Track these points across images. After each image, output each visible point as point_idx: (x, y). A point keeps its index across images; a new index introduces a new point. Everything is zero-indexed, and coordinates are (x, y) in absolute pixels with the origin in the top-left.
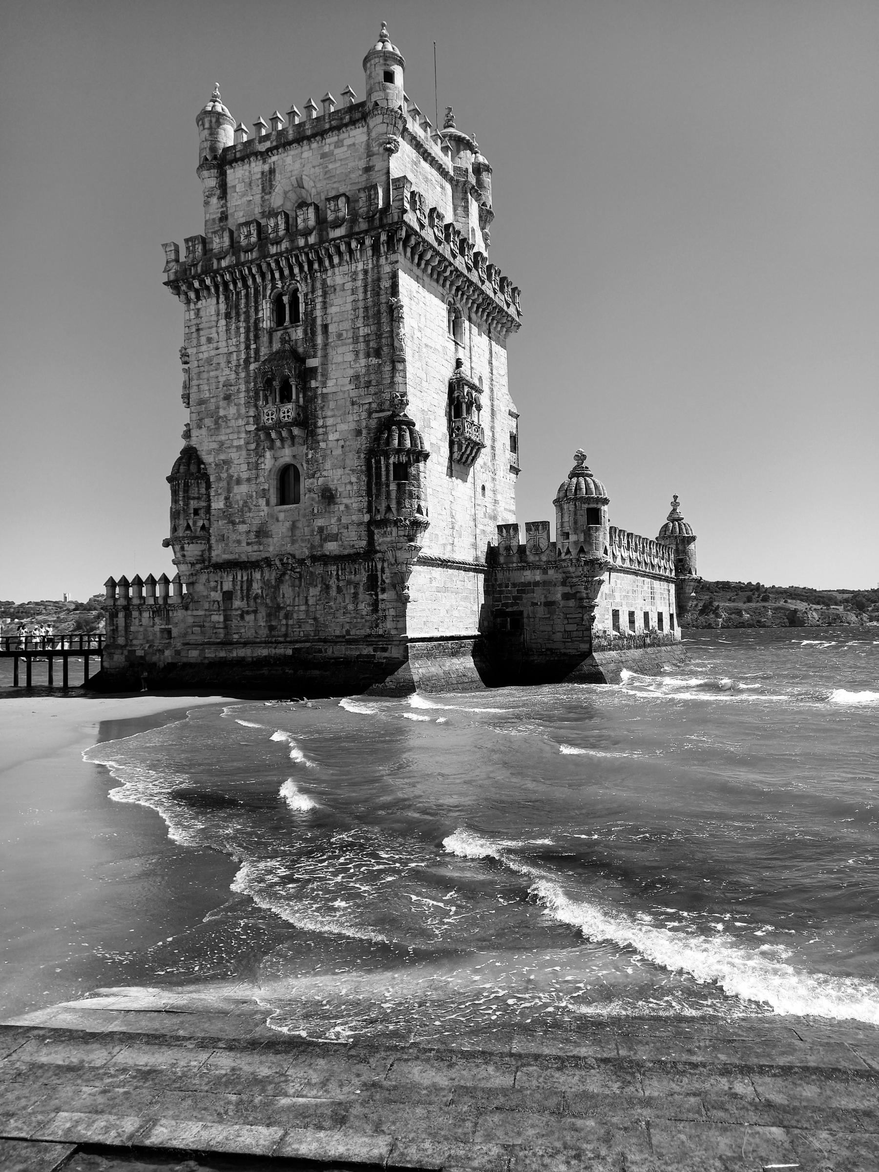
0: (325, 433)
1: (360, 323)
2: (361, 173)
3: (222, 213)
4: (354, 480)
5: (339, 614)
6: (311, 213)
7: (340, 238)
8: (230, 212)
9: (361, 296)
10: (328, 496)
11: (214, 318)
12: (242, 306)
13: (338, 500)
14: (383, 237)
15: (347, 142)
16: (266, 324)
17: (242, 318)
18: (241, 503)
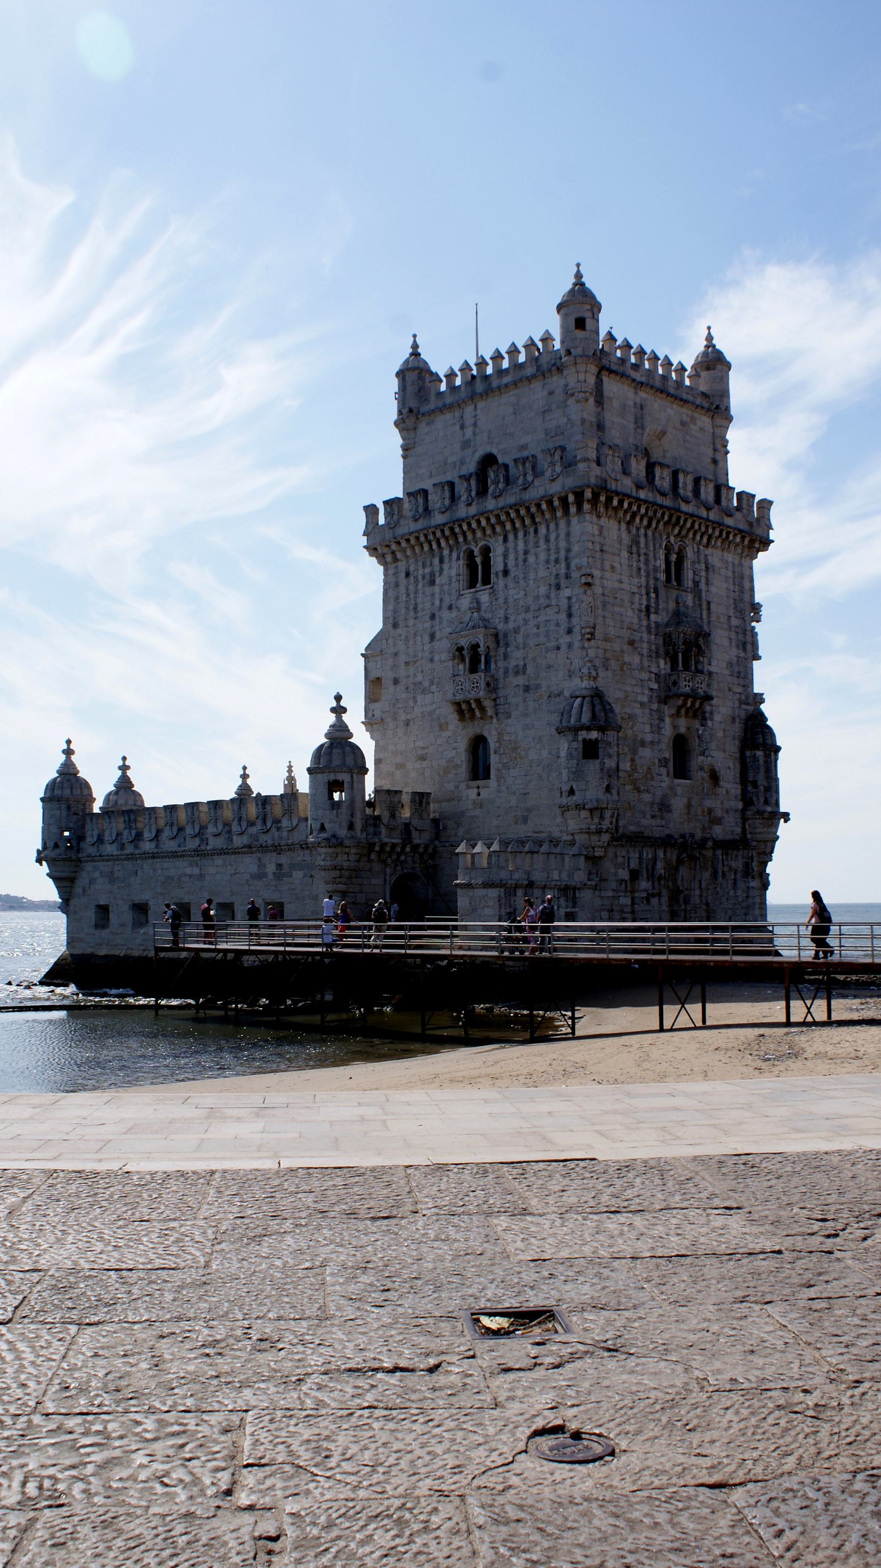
0: (711, 713)
1: (731, 613)
2: (709, 460)
3: (599, 421)
4: (731, 765)
5: (724, 899)
6: (711, 487)
7: (735, 529)
8: (608, 424)
9: (731, 587)
10: (714, 777)
11: (617, 546)
12: (642, 545)
13: (721, 783)
14: (757, 545)
15: (699, 423)
16: (662, 577)
17: (642, 558)
18: (645, 768)
